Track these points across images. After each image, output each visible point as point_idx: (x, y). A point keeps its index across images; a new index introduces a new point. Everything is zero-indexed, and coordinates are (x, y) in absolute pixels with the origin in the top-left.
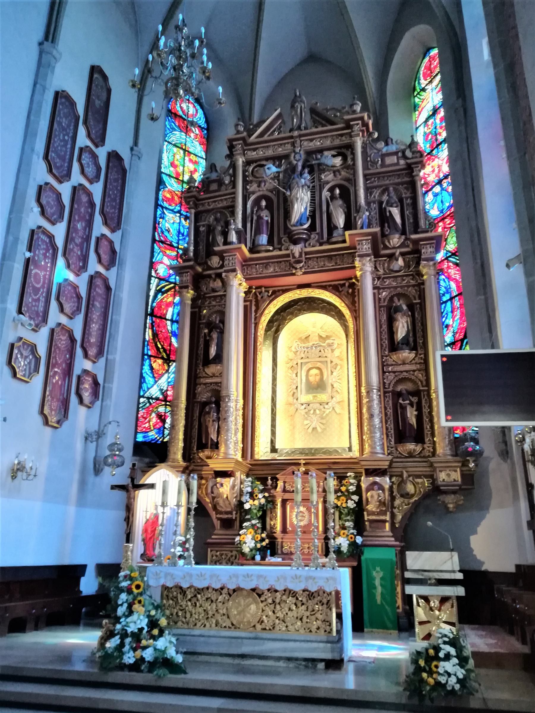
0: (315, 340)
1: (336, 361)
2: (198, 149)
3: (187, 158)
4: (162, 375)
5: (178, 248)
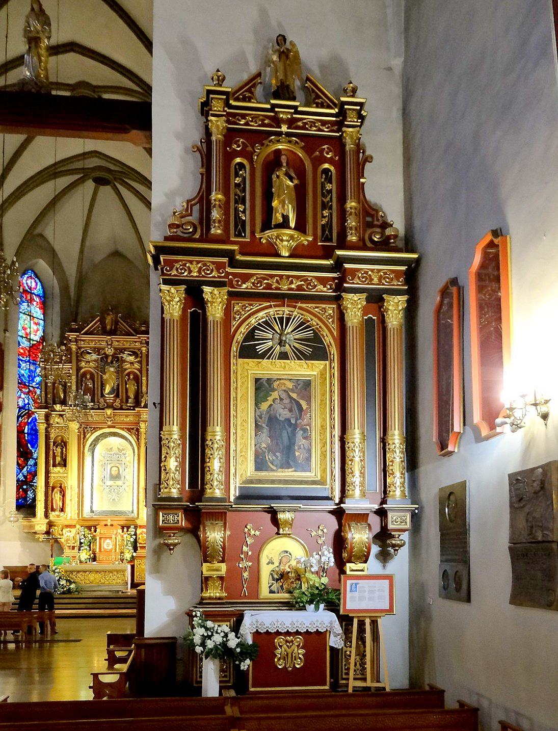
0: (115, 450)
1: (127, 463)
2: (37, 312)
3: (32, 322)
4: (25, 466)
5: (29, 386)
